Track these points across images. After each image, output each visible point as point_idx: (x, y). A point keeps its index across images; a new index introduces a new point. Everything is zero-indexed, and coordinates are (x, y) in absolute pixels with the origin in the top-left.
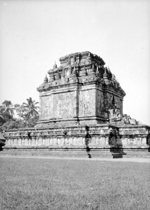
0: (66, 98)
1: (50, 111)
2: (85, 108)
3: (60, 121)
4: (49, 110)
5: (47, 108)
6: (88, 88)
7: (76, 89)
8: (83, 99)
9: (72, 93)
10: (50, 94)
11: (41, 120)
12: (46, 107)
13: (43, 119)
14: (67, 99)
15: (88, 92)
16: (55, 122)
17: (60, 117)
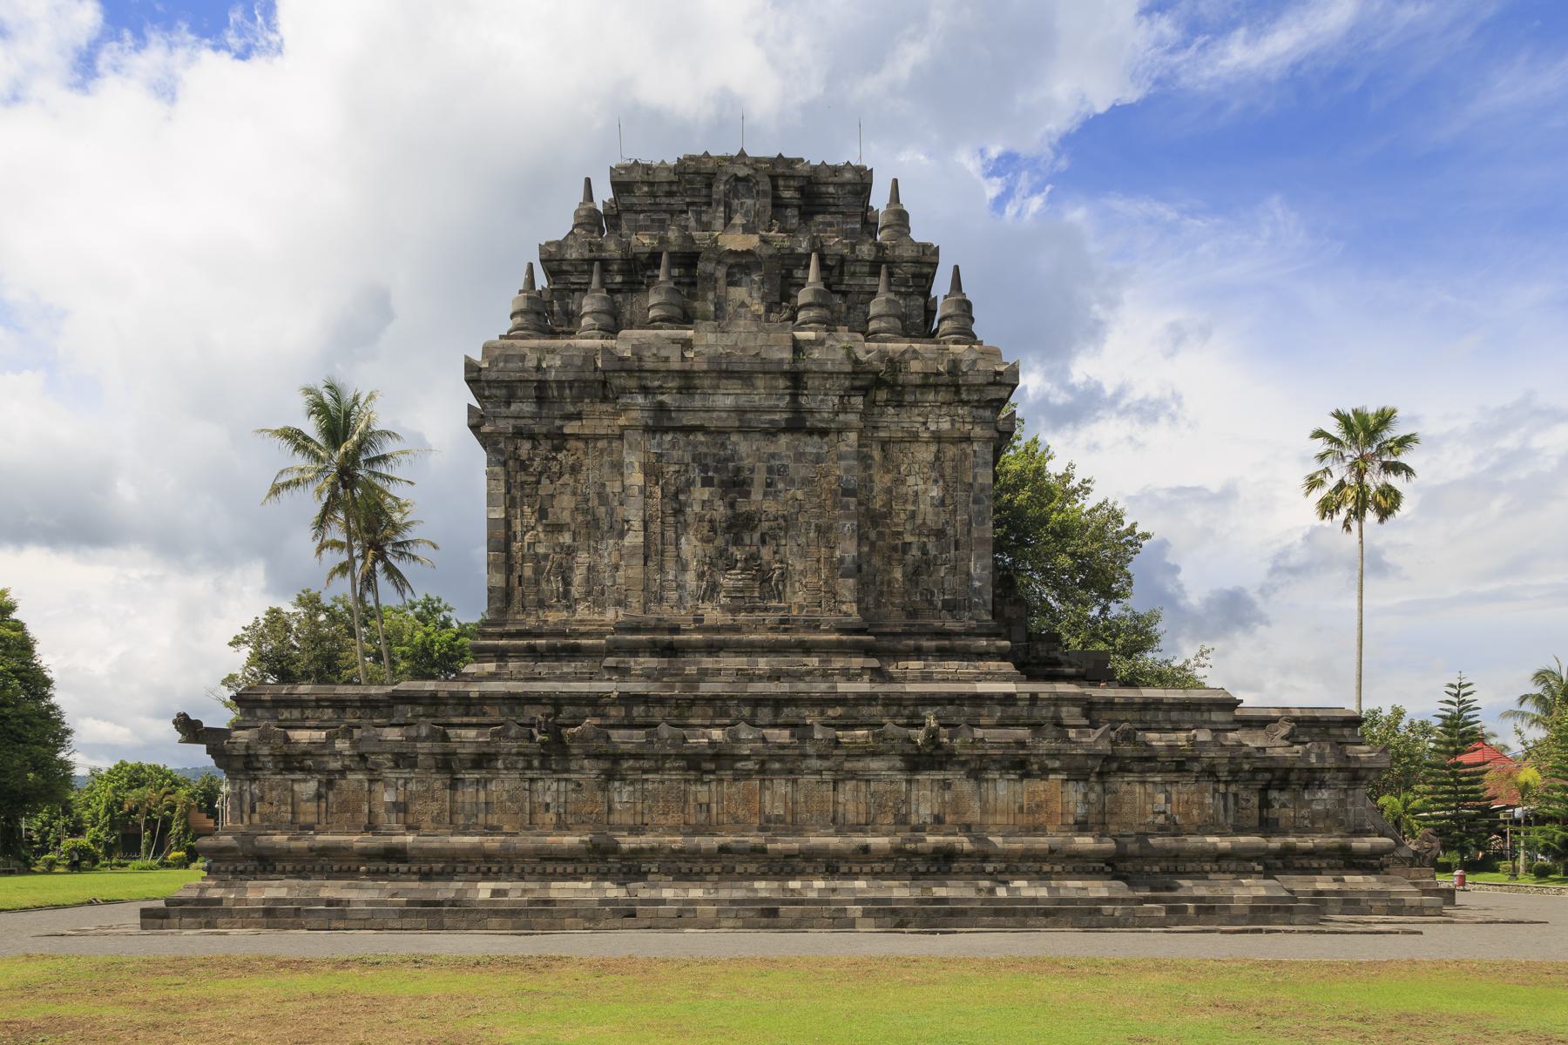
0: (760, 477)
1: (591, 569)
2: (910, 569)
3: (712, 649)
4: (583, 557)
5: (566, 538)
6: (933, 427)
7: (853, 418)
8: (888, 504)
9: (811, 445)
10: (603, 426)
11: (512, 628)
12: (557, 528)
13: (531, 622)
14: (769, 485)
15: (937, 458)
16: (670, 650)
17: (713, 614)
